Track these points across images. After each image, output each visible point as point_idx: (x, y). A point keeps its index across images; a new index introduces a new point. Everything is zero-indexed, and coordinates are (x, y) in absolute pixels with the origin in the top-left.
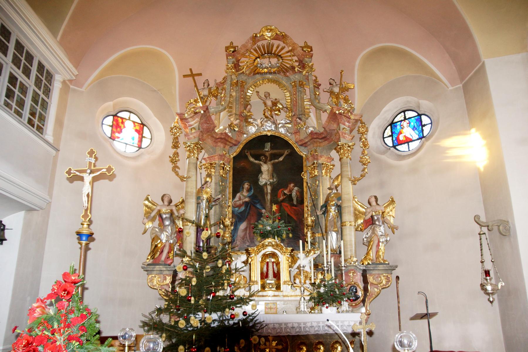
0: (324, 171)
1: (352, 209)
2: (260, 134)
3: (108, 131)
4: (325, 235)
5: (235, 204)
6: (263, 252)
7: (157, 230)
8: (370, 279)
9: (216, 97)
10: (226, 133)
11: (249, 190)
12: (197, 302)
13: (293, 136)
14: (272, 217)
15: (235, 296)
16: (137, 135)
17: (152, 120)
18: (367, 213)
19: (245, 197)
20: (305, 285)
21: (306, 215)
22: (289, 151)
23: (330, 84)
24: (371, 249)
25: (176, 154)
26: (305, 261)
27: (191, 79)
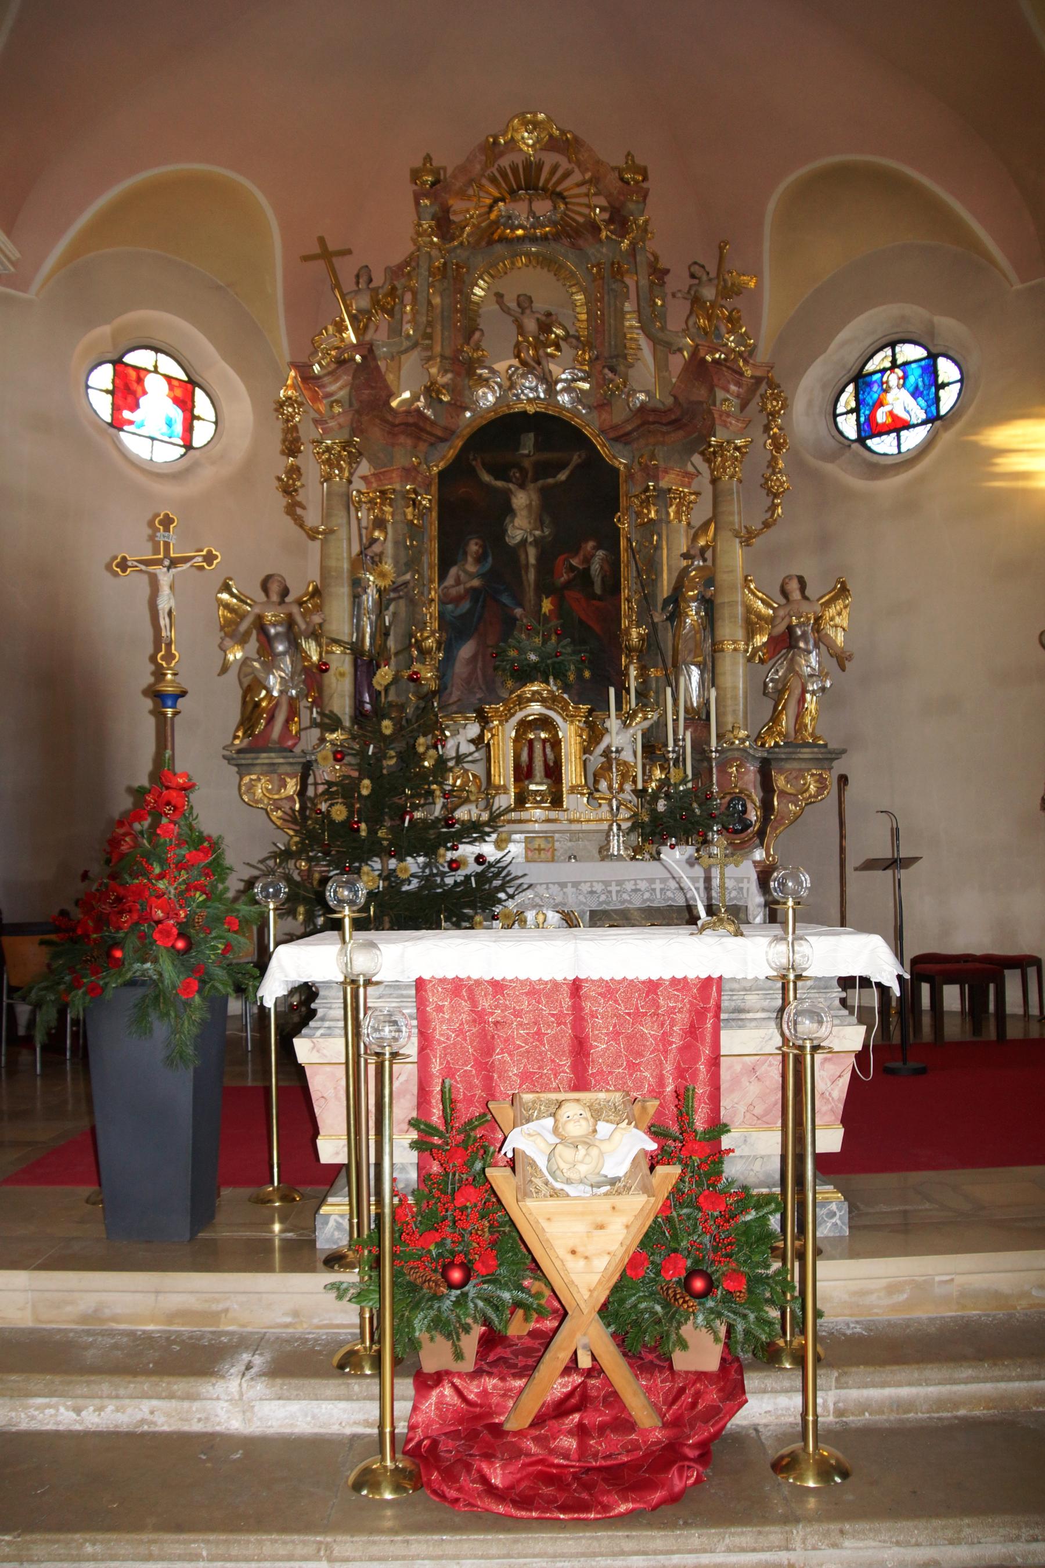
0: (672, 510)
1: (740, 610)
2: (505, 410)
3: (102, 405)
4: (672, 676)
5: (445, 595)
6: (520, 715)
7: (256, 664)
8: (780, 782)
9: (391, 313)
10: (418, 410)
11: (480, 559)
12: (372, 832)
13: (595, 414)
14: (541, 628)
15: (458, 821)
16: (177, 415)
17: (219, 369)
18: (778, 620)
19: (471, 576)
20: (621, 796)
21: (625, 623)
22: (584, 456)
23: (693, 276)
24: (784, 708)
25: (294, 471)
26: (623, 738)
27: (320, 265)
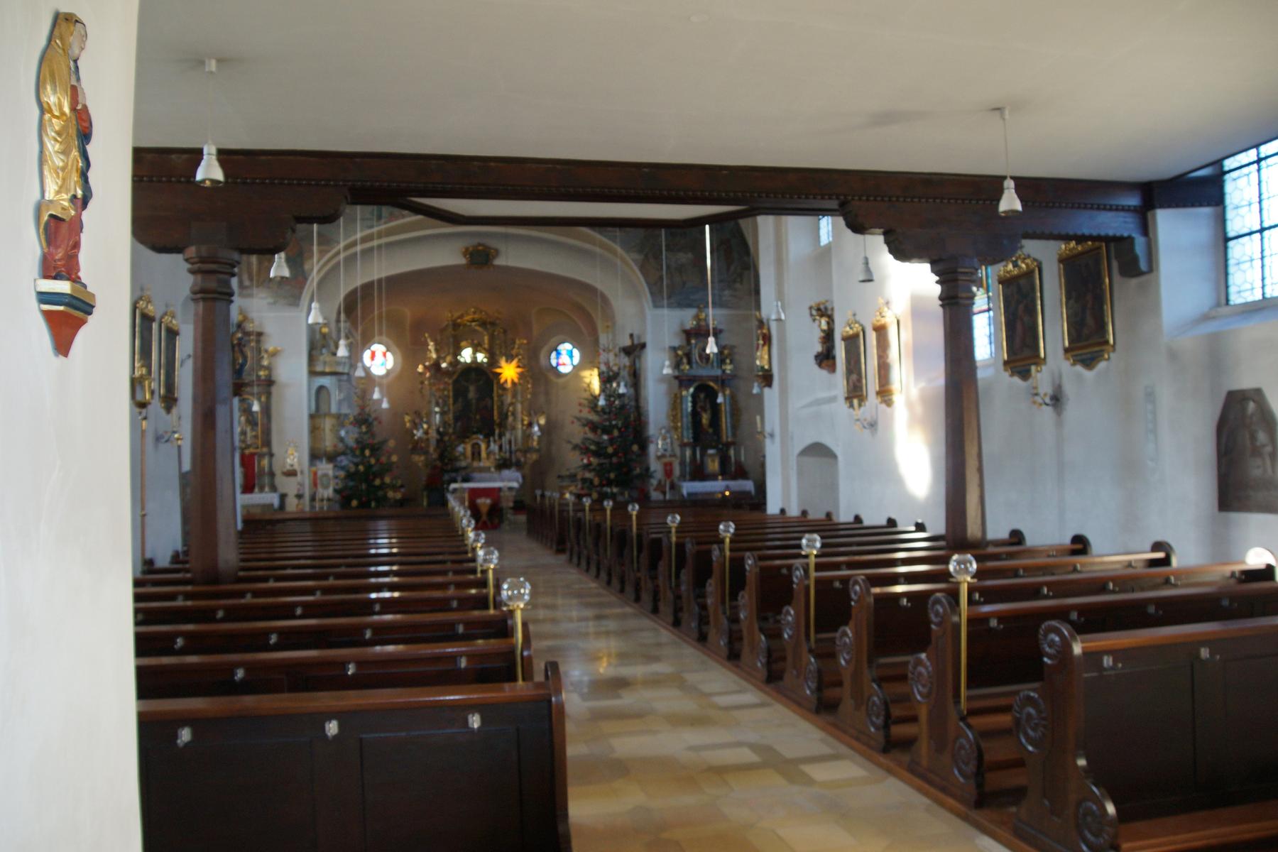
26: (494, 447)
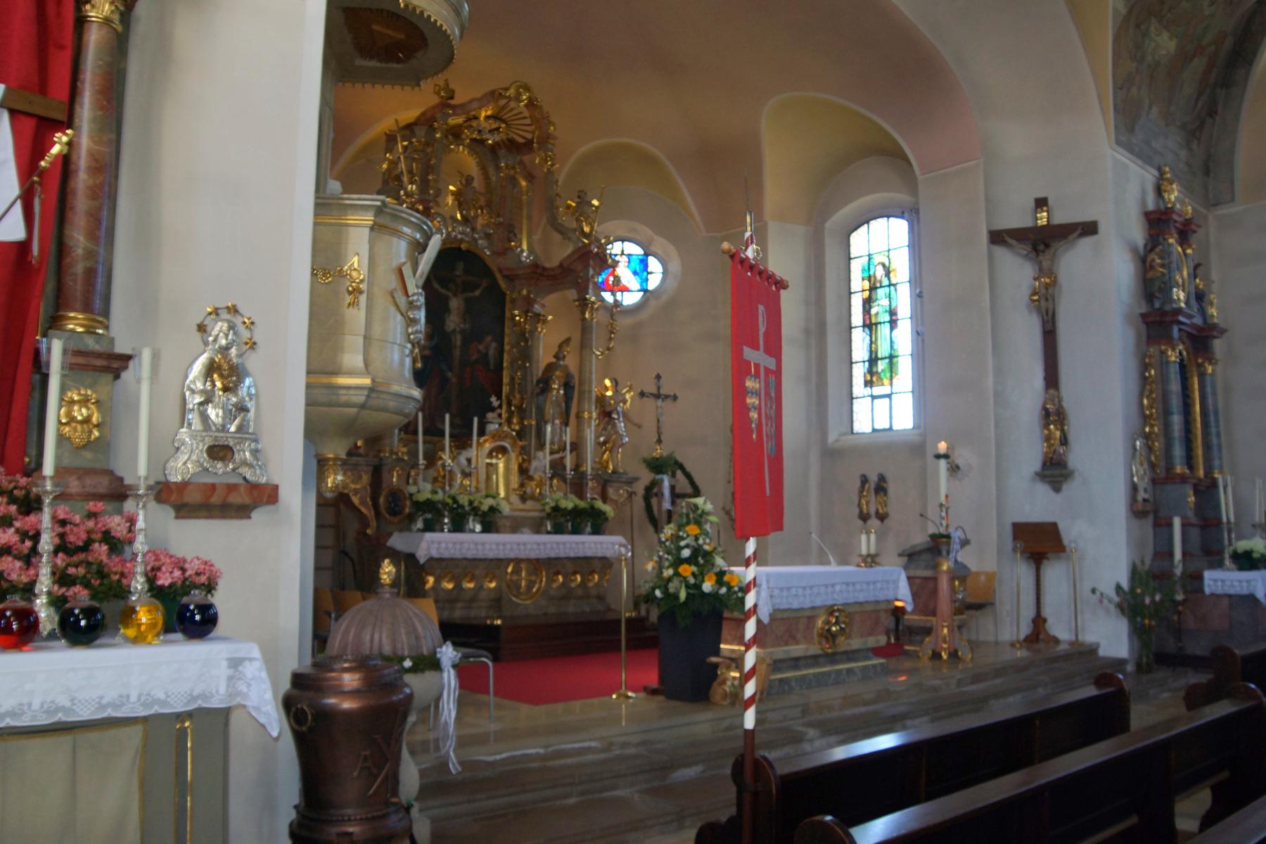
8: (611, 491)
